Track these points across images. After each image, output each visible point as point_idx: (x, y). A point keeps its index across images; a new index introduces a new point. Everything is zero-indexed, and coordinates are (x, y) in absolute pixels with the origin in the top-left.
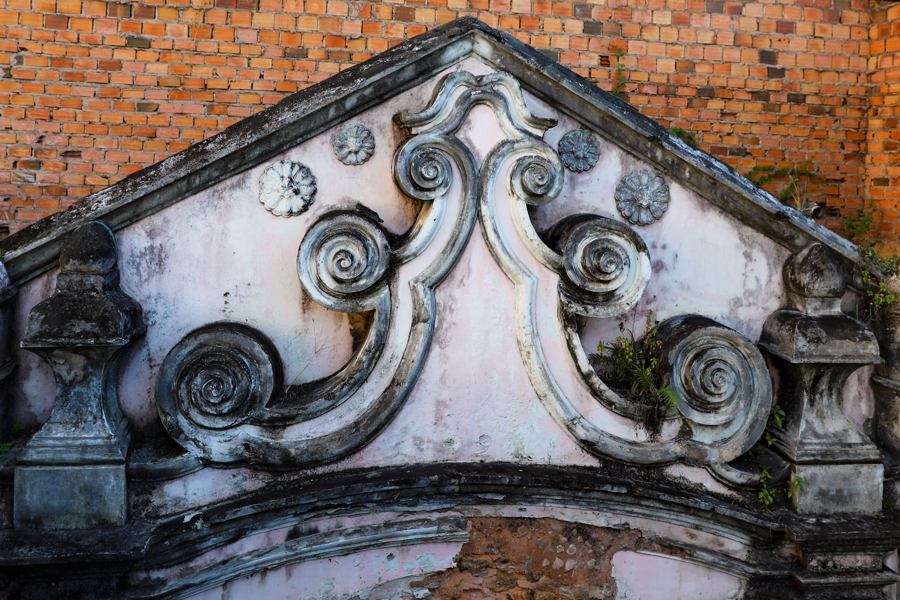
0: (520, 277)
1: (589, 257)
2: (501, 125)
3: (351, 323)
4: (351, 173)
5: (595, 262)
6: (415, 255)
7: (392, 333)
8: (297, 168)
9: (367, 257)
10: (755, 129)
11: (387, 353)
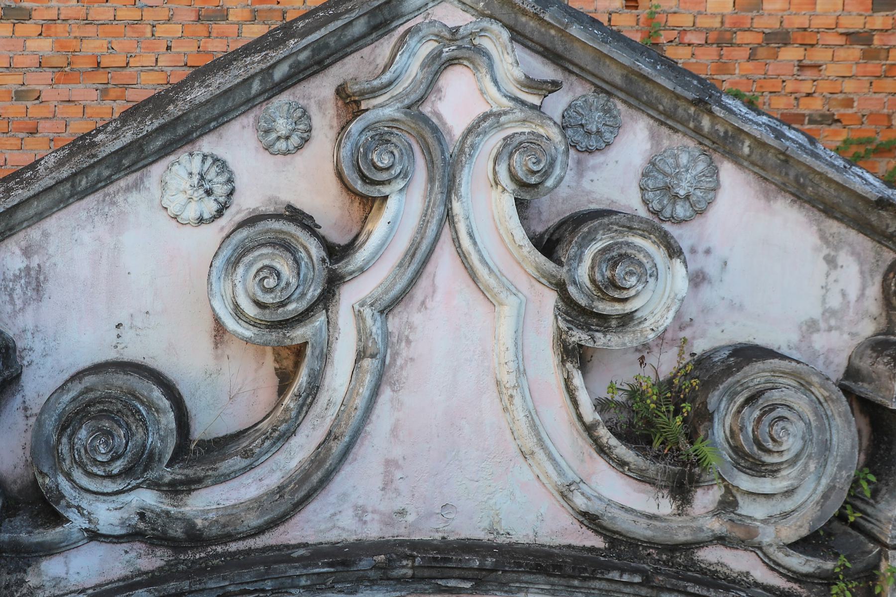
1: (600, 266)
3: (276, 360)
4: (279, 165)
5: (608, 274)
6: (362, 270)
7: (329, 372)
8: (209, 161)
9: (299, 274)
10: (849, 86)
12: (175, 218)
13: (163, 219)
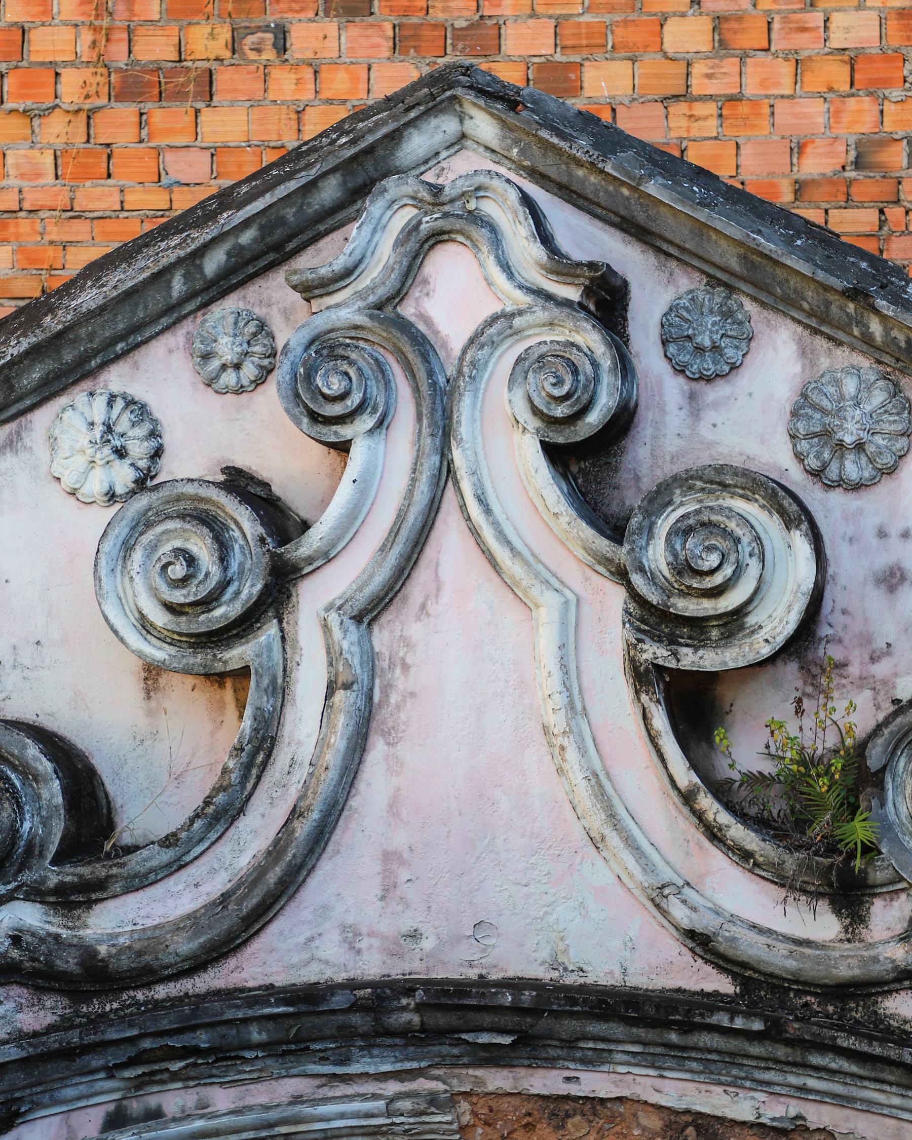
0: (535, 591)
2: (489, 283)
11: (282, 757)
12: (73, 493)
13: (55, 495)
